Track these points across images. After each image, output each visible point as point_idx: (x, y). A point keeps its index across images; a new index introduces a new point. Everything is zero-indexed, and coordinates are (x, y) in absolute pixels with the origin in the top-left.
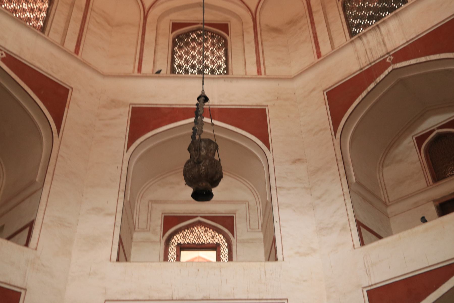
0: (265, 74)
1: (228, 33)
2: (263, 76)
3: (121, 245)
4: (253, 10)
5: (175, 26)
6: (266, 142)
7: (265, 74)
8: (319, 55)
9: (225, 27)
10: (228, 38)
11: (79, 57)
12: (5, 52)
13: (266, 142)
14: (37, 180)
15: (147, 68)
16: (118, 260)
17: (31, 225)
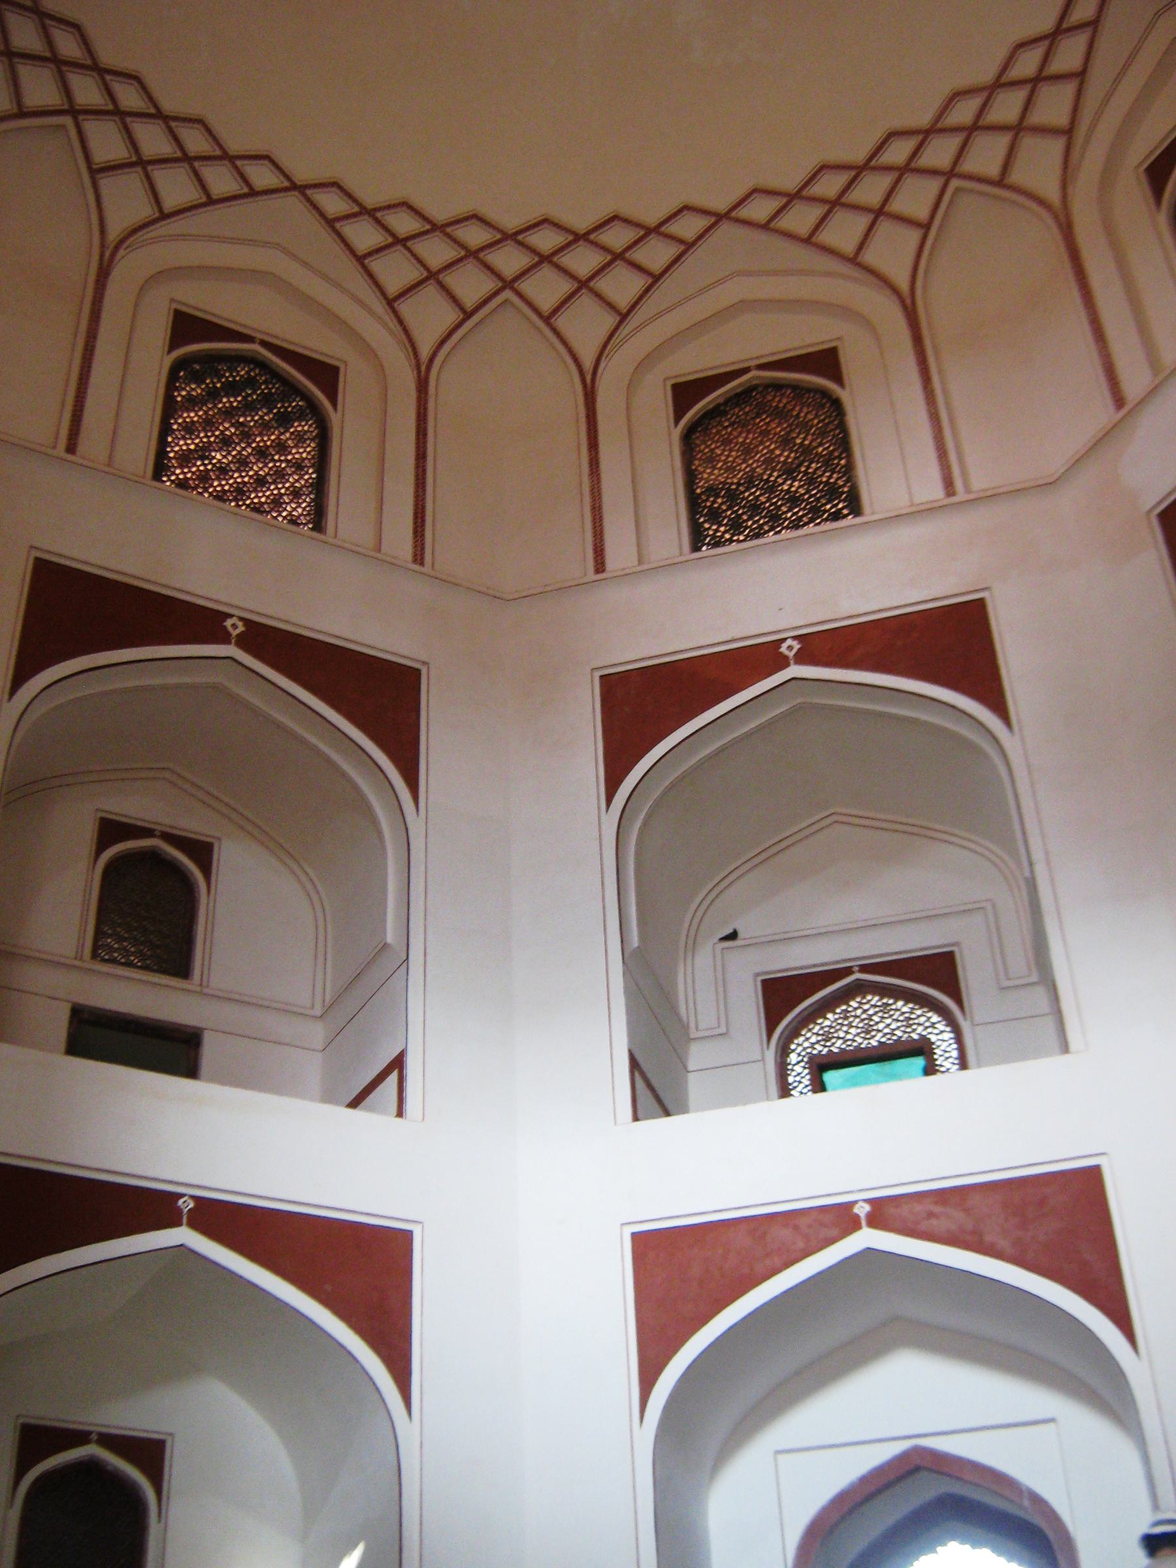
0: (968, 490)
1: (838, 378)
2: (961, 496)
3: (637, 1074)
4: (904, 286)
5: (685, 393)
6: (998, 705)
7: (968, 490)
8: (1119, 400)
9: (826, 361)
10: (844, 395)
11: (427, 569)
12: (241, 619)
13: (998, 705)
14: (390, 939)
15: (619, 554)
16: (636, 1118)
17: (398, 1063)
